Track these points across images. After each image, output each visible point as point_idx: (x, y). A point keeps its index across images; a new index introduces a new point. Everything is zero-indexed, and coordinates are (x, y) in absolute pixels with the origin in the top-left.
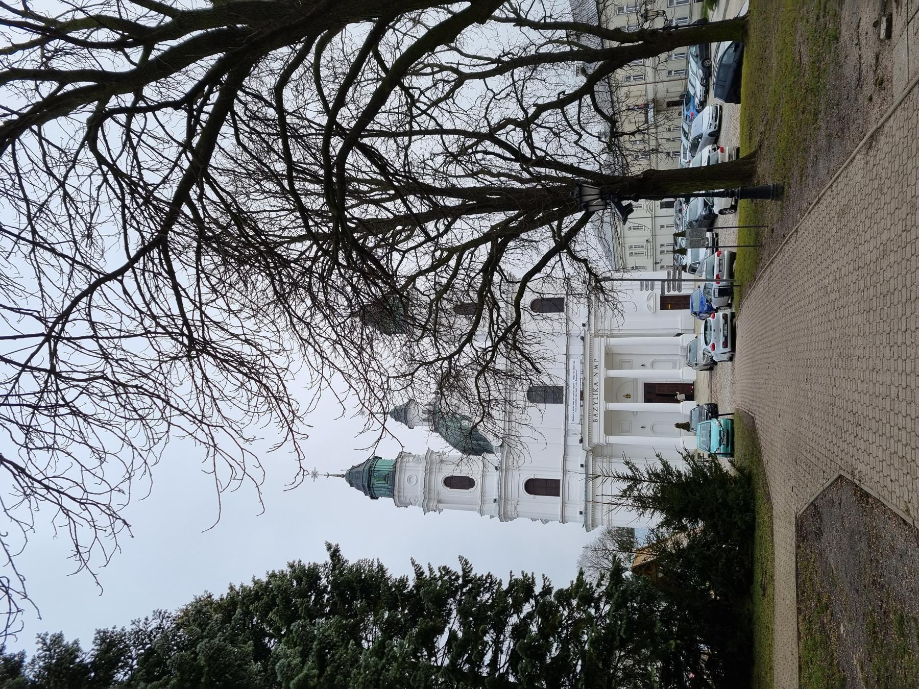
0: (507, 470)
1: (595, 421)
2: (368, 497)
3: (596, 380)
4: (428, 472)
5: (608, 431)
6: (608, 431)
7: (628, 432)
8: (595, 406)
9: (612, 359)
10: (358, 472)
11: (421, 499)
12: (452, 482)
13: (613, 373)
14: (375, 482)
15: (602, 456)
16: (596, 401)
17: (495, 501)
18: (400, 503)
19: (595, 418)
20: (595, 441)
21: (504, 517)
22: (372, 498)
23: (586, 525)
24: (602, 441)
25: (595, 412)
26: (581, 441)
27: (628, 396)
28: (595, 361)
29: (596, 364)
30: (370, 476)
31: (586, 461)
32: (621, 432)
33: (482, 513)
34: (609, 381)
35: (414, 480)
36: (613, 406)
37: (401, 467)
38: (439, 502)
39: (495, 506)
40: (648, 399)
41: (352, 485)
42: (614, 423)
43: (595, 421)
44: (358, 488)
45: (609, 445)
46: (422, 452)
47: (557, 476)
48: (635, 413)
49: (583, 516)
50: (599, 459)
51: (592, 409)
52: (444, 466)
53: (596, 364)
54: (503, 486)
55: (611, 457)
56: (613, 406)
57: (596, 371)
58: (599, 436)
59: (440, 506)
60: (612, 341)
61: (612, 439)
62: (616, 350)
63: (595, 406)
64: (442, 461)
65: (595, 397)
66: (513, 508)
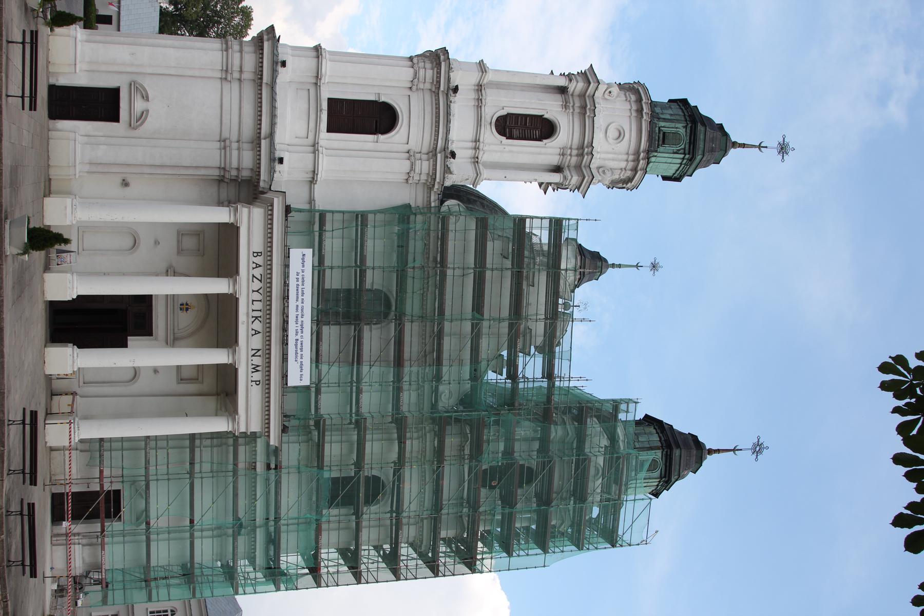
0: (433, 153)
2: (692, 103)
3: (257, 342)
4: (585, 149)
5: (229, 232)
6: (229, 232)
7: (184, 232)
8: (257, 285)
9: (221, 387)
10: (712, 150)
11: (598, 94)
12: (539, 128)
13: (219, 357)
14: (682, 131)
16: (257, 296)
17: (456, 90)
18: (634, 91)
19: (259, 260)
20: (258, 213)
21: (438, 58)
22: (684, 102)
23: (275, 40)
24: (244, 211)
25: (258, 272)
27: (185, 307)
28: (257, 383)
29: (257, 376)
30: (693, 142)
31: (272, 171)
32: (199, 231)
33: (482, 66)
35: (613, 133)
36: (218, 286)
37: (637, 160)
38: (562, 90)
39: (457, 78)
40: (146, 301)
41: (721, 127)
42: (217, 250)
43: (258, 254)
44: (707, 122)
46: (597, 190)
48: (171, 271)
50: (246, 174)
51: (267, 279)
52: (555, 160)
53: (257, 376)
54: (441, 118)
55: (221, 180)
56: (218, 286)
57: (257, 361)
58: (250, 222)
59: (562, 82)
61: (221, 215)
62: (211, 402)
63: (257, 285)
64: (558, 169)
65: (258, 306)
66: (422, 72)
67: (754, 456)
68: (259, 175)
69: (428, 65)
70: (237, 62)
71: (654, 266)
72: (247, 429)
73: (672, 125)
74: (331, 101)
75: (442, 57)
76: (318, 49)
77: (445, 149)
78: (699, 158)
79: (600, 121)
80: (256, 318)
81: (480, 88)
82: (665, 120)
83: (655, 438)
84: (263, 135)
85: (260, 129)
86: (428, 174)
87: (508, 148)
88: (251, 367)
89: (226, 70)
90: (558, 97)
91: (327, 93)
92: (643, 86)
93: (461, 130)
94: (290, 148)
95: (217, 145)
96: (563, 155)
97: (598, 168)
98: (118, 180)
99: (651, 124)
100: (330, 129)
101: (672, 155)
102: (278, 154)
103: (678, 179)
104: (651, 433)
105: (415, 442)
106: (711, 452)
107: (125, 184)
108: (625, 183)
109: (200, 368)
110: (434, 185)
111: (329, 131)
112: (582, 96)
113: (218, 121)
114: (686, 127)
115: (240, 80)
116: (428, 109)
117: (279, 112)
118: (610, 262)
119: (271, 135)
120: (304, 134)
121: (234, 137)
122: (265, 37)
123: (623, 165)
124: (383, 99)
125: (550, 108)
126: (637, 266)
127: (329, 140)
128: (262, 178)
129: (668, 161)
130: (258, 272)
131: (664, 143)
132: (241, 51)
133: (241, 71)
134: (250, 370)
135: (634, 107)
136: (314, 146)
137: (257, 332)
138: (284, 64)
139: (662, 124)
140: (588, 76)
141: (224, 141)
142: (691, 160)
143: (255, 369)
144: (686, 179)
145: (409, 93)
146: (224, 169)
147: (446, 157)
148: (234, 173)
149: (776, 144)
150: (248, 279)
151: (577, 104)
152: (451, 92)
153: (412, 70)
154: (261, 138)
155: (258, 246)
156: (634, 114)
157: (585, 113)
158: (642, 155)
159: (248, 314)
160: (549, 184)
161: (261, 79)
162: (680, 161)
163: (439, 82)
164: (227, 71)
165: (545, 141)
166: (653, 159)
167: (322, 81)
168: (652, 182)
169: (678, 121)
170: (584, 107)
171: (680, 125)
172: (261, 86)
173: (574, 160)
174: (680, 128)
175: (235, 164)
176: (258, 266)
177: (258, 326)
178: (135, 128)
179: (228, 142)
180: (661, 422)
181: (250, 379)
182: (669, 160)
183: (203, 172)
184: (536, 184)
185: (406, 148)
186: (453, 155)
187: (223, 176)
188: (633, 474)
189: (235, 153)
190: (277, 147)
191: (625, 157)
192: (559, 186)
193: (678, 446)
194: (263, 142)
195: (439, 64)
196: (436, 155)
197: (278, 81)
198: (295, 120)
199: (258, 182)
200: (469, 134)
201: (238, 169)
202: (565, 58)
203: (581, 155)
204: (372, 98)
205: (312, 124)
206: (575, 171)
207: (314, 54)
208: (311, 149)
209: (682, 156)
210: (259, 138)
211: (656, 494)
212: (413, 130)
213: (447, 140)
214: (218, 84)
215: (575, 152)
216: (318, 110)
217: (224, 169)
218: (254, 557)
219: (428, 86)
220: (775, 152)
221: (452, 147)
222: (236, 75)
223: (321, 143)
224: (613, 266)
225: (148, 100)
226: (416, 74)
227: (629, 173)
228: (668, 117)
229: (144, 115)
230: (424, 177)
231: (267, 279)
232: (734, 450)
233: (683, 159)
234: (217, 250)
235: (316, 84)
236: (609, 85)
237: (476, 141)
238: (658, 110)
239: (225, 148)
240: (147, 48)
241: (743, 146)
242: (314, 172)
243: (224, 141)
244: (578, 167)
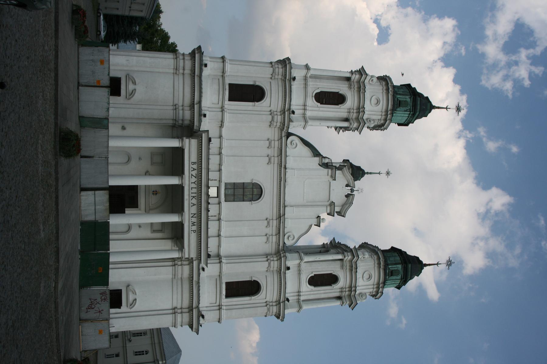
0: (283, 112)
1: (194, 163)
3: (194, 210)
4: (360, 109)
5: (179, 152)
9: (176, 233)
11: (366, 81)
12: (337, 99)
14: (409, 100)
15: (181, 126)
16: (193, 185)
17: (294, 79)
18: (385, 80)
19: (195, 166)
20: (194, 142)
21: (285, 63)
22: (409, 85)
23: (201, 54)
24: (187, 141)
26: (210, 140)
27: (155, 193)
29: (194, 228)
31: (200, 121)
33: (307, 67)
34: (178, 208)
35: (374, 101)
36: (174, 181)
37: (387, 115)
38: (348, 79)
39: (295, 73)
40: (134, 189)
41: (427, 98)
42: (173, 161)
43: (194, 163)
44: (421, 95)
45: (180, 137)
47: (231, 106)
48: (147, 173)
49: (205, 62)
50: (187, 122)
51: (199, 176)
52: (345, 115)
54: (287, 94)
55: (174, 126)
56: (174, 181)
57: (194, 220)
58: (190, 147)
59: (348, 75)
60: (176, 255)
61: (174, 143)
66: (277, 70)
67: (447, 267)
68: (194, 123)
69: (280, 66)
70: (181, 64)
71: (388, 173)
72: (189, 256)
73: (404, 97)
74: (231, 85)
75: (287, 62)
76: (223, 58)
77: (289, 109)
78: (417, 113)
79: (368, 95)
80: (194, 197)
81: (305, 78)
82: (400, 94)
83: (398, 258)
84: (195, 103)
85: (194, 99)
86: (281, 122)
87: (321, 109)
88: (191, 223)
89: (176, 69)
90: (346, 82)
91: (228, 81)
92: (389, 77)
93: (296, 101)
94: (210, 109)
95: (172, 108)
96: (349, 112)
97: (367, 119)
98: (120, 126)
99: (394, 97)
100: (230, 100)
101: (404, 112)
102: (203, 112)
103: (406, 124)
104: (395, 256)
105: (276, 263)
106: (426, 265)
107: (124, 128)
108: (380, 127)
109: (163, 224)
110: (284, 128)
111: (229, 100)
112: (358, 82)
113: (172, 95)
114: (410, 98)
115: (183, 74)
116: (280, 88)
117: (204, 90)
118: (366, 171)
119: (200, 102)
120: (216, 101)
121: (181, 104)
122: (196, 52)
123: (379, 117)
124: (257, 84)
125: (342, 88)
126: (379, 173)
128: (195, 124)
129: (401, 115)
130: (194, 173)
131: (399, 106)
132: (184, 59)
133: (184, 69)
134: (191, 225)
135: (385, 88)
136: (222, 108)
137: (194, 205)
138: (206, 65)
139: (398, 96)
140: (361, 72)
141: (175, 105)
142: (414, 115)
143: (193, 224)
144: (410, 125)
145: (270, 80)
146: (175, 120)
147: (290, 114)
148: (180, 122)
149: (455, 107)
150: (189, 176)
151: (356, 86)
152: (292, 80)
153: (272, 69)
154: (195, 104)
155: (194, 158)
156: (385, 91)
157: (360, 91)
158: (389, 112)
159: (189, 195)
160: (341, 128)
161: (194, 73)
162: (407, 115)
163: (286, 75)
164: (176, 69)
165: (340, 105)
166: (394, 115)
167: (226, 75)
168: (393, 126)
169: (407, 95)
170: (359, 88)
171: (407, 97)
172: (194, 77)
173: (355, 115)
174: (408, 99)
175: (181, 117)
176: (194, 169)
177: (194, 201)
178: (129, 99)
179: (177, 106)
180: (400, 250)
181: (190, 229)
182: (403, 115)
183: (164, 122)
184: (333, 129)
185: (269, 109)
186: (293, 112)
187: (175, 124)
188: (387, 277)
189: (181, 112)
190: (203, 108)
191: (381, 113)
192: (346, 129)
193: (410, 263)
194: (196, 106)
195: (286, 66)
196: (284, 113)
197: (203, 74)
198: (211, 96)
199: (193, 127)
200: (301, 102)
201: (183, 120)
202: (346, 66)
203: (359, 112)
204: (251, 83)
205: (221, 97)
206: (355, 122)
207: (221, 60)
208: (221, 109)
209: (409, 113)
210: (193, 104)
211: (399, 287)
212: (272, 101)
213: (290, 105)
214: (172, 76)
215: (355, 111)
216: (224, 89)
217: (175, 120)
218: (192, 325)
219: (280, 77)
220: (455, 111)
221: (293, 108)
222: (181, 71)
223: (226, 106)
224: (368, 173)
225: (135, 84)
226: (274, 71)
227: (382, 122)
228: (401, 93)
229: (133, 92)
230: (279, 124)
231: (199, 176)
232: (437, 264)
233: (409, 114)
234: (173, 161)
235: (223, 76)
236: (372, 76)
237: (305, 106)
238: (396, 89)
239: (176, 109)
240: (135, 58)
241: (439, 108)
242: (222, 121)
243: (175, 105)
244: (357, 119)
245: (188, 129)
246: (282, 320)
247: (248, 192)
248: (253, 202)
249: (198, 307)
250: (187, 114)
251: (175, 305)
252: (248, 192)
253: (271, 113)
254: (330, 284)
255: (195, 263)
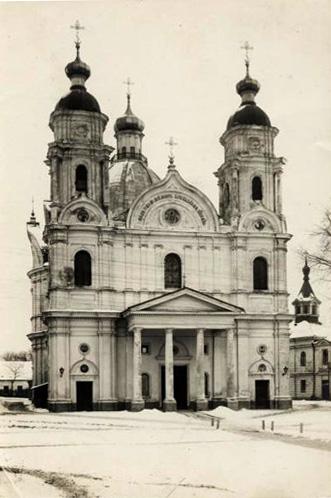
5: (144, 332)
12: (81, 173)
15: (117, 329)
36: (169, 337)
55: (117, 336)
56: (169, 337)
58: (140, 323)
89: (66, 334)
127: (95, 283)
175: (109, 330)
189: (105, 329)
234: (153, 340)
245: (121, 324)
246: (291, 236)
247: (173, 263)
248: (182, 261)
249: (275, 316)
250: (106, 324)
251: (271, 335)
252: (173, 263)
253: (100, 244)
254: (260, 183)
255: (237, 318)
